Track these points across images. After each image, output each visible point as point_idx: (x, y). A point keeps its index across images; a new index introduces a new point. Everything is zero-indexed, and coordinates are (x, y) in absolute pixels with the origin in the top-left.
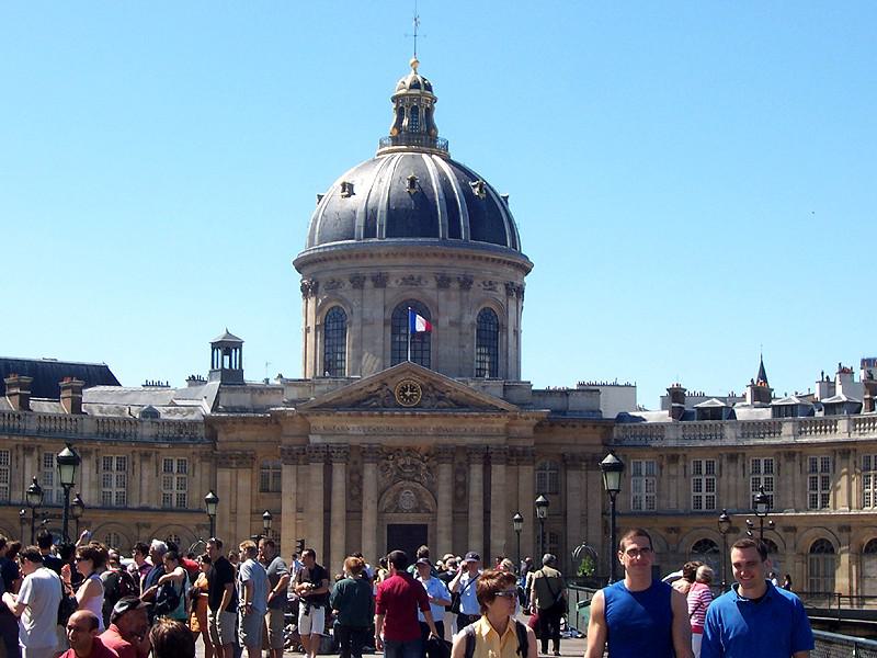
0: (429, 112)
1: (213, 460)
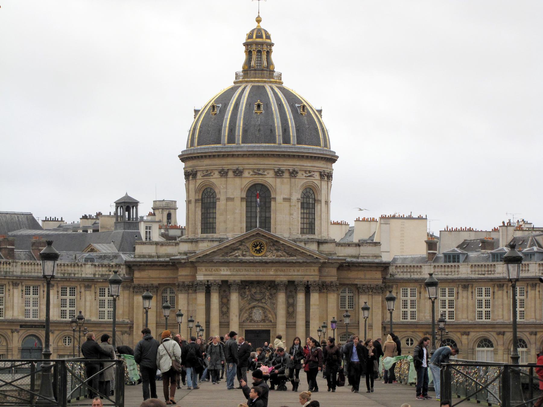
0: (269, 53)
1: (131, 289)
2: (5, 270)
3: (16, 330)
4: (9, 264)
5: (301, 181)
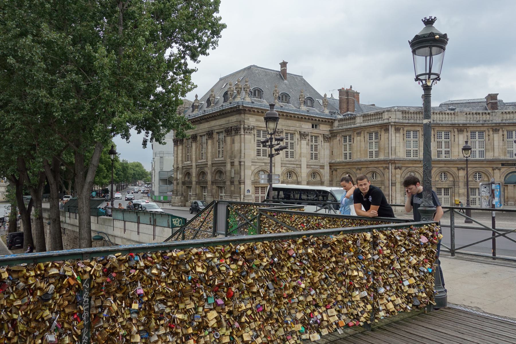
2: (485, 119)
3: (497, 168)
4: (489, 114)
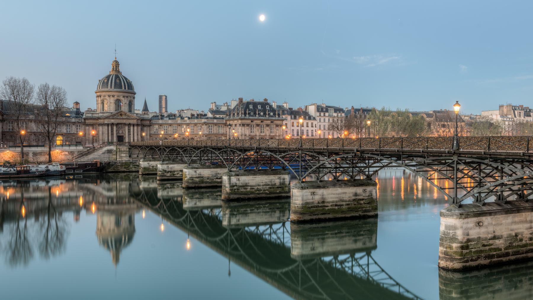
5: (129, 99)
